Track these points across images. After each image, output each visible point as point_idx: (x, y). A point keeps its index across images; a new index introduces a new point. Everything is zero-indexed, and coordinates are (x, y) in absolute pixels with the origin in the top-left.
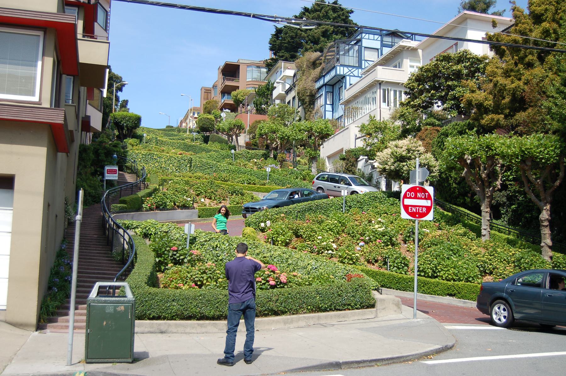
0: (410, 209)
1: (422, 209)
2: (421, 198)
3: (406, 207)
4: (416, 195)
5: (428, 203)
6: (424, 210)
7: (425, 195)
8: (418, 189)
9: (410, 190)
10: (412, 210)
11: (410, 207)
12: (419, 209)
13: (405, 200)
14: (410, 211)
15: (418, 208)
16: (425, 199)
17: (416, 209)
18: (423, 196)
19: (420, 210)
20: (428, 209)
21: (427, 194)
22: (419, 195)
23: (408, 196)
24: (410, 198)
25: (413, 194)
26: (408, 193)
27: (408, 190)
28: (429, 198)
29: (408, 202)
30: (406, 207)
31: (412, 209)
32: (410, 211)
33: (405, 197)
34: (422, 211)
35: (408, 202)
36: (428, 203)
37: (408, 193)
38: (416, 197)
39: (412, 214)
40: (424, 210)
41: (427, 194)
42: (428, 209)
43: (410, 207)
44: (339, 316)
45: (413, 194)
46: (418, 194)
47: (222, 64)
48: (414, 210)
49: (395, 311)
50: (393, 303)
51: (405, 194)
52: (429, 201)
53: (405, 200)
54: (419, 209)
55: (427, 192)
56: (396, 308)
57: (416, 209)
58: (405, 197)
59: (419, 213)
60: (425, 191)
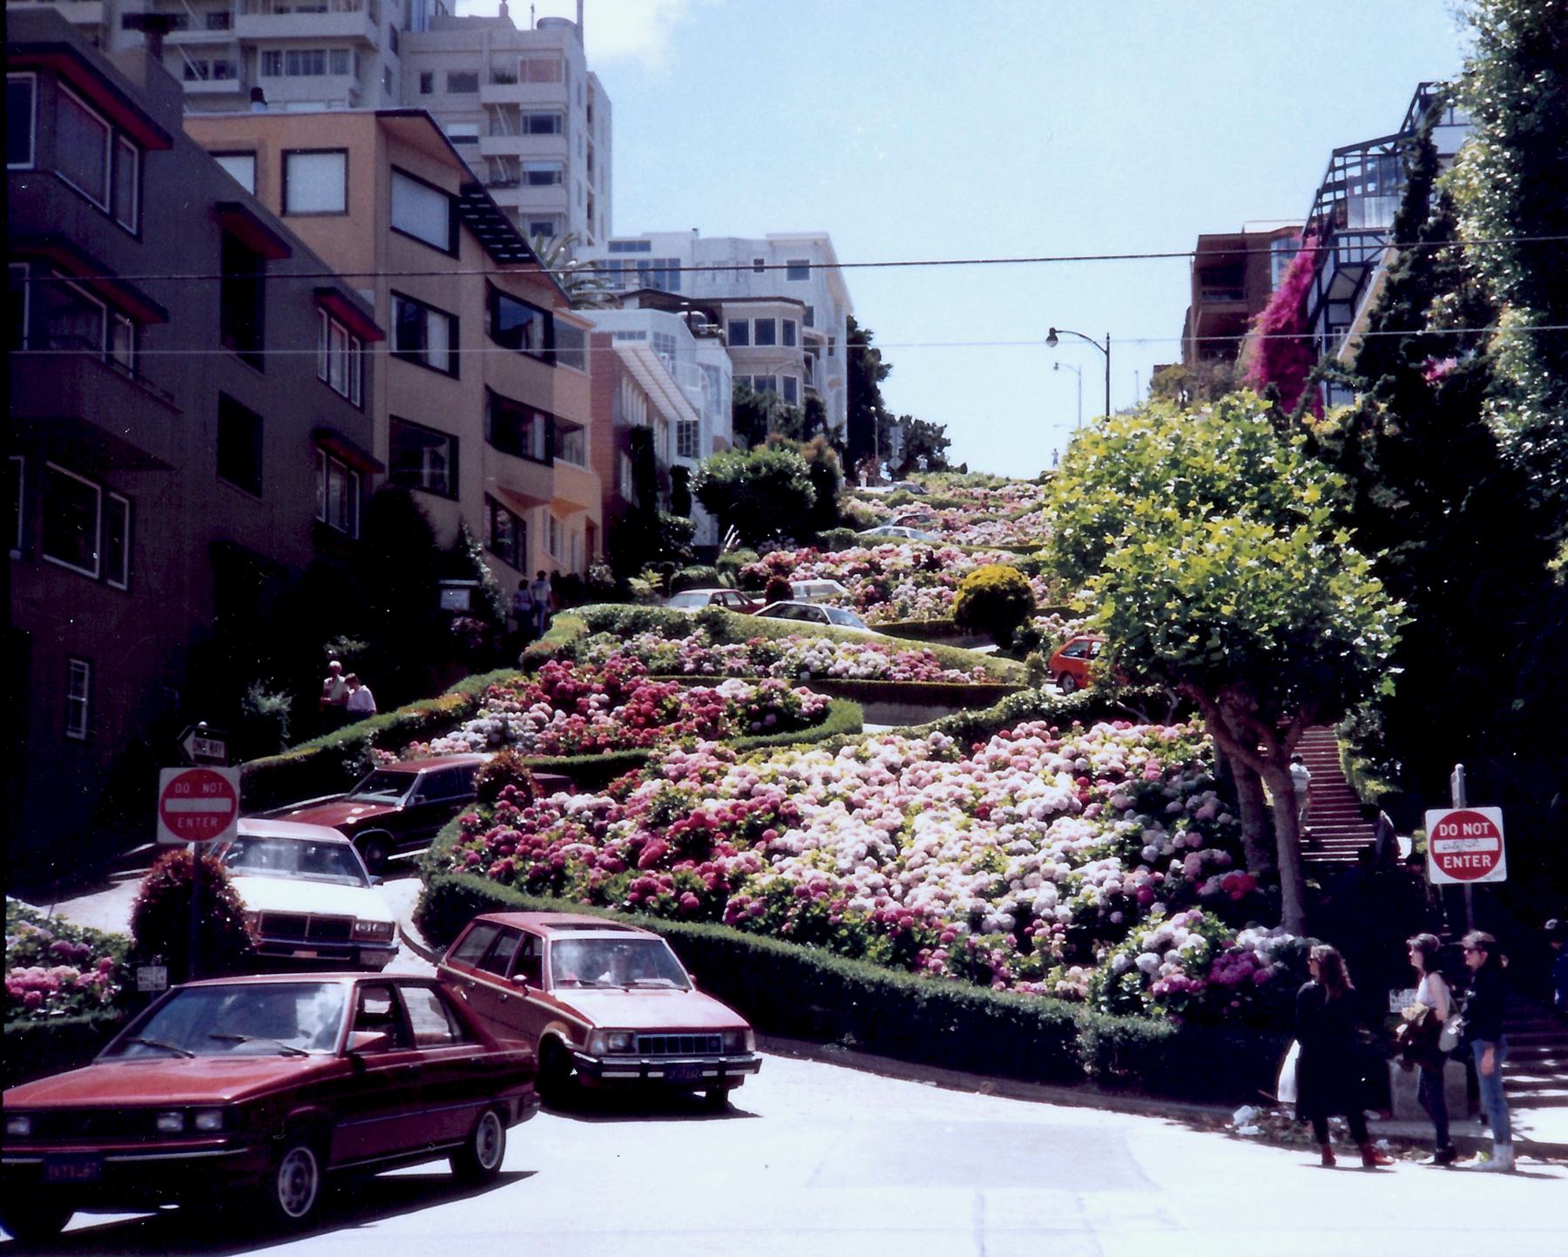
2: (1474, 836)
4: (1460, 830)
5: (1491, 844)
6: (1486, 860)
9: (1447, 820)
12: (1471, 860)
15: (1467, 858)
16: (1483, 836)
17: (1464, 861)
18: (1477, 830)
19: (1475, 861)
20: (1494, 856)
21: (1486, 824)
22: (1467, 828)
24: (1448, 837)
28: (1492, 832)
30: (1439, 858)
33: (1436, 835)
36: (1491, 844)
38: (1461, 836)
48: (1458, 862)
54: (1471, 860)
57: (1464, 861)
58: (1436, 835)
60: (1482, 819)
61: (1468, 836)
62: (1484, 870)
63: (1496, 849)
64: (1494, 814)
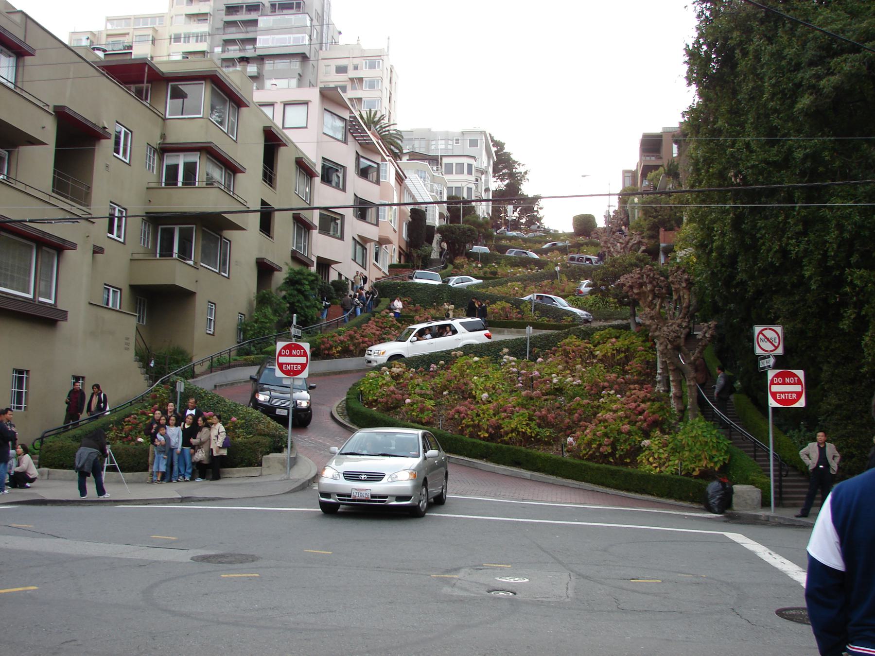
2: (296, 356)
3: (281, 366)
4: (291, 352)
5: (303, 360)
6: (299, 367)
8: (293, 346)
9: (285, 348)
13: (280, 358)
16: (300, 356)
20: (304, 366)
21: (302, 351)
22: (294, 352)
24: (285, 355)
27: (283, 348)
28: (305, 355)
29: (282, 360)
30: (281, 366)
33: (280, 355)
35: (282, 360)
36: (303, 360)
38: (291, 355)
39: (286, 372)
40: (299, 367)
42: (304, 366)
47: (640, 137)
48: (288, 367)
50: (279, 462)
51: (281, 351)
52: (305, 358)
53: (280, 357)
55: (303, 348)
56: (281, 467)
60: (301, 348)
61: (294, 356)
62: (299, 372)
63: (305, 362)
64: (306, 346)
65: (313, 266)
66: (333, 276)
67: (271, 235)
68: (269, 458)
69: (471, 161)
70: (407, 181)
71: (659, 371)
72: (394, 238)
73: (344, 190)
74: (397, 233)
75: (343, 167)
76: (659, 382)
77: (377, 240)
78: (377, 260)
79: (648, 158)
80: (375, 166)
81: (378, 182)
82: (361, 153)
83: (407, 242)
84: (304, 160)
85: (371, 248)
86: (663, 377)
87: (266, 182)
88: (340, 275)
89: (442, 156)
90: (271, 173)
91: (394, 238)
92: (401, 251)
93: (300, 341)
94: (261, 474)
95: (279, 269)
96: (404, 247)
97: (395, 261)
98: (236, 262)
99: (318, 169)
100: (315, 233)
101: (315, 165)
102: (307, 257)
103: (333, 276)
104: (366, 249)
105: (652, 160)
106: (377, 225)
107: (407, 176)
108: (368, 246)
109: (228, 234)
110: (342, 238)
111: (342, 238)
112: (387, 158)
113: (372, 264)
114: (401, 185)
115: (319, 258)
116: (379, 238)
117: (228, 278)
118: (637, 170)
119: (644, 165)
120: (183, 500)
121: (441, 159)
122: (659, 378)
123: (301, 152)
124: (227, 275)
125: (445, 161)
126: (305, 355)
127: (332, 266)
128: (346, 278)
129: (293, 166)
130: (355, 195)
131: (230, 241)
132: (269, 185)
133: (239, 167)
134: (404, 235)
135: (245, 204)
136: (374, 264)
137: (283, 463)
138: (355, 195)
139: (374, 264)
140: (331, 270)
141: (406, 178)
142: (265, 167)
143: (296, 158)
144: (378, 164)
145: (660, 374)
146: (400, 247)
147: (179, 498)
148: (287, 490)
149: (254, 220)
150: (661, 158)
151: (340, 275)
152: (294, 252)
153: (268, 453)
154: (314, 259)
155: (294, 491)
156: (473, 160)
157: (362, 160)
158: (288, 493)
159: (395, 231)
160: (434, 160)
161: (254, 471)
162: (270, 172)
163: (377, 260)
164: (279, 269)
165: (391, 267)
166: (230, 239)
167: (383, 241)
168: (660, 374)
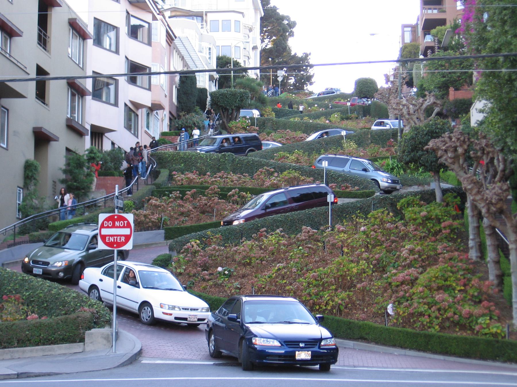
0: (107, 239)
1: (120, 238)
2: (120, 227)
5: (127, 231)
6: (123, 239)
7: (124, 223)
8: (116, 217)
9: (107, 219)
10: (109, 240)
11: (107, 237)
12: (117, 239)
13: (103, 230)
14: (107, 241)
15: (115, 237)
16: (124, 227)
17: (114, 239)
18: (122, 224)
19: (118, 239)
20: (127, 238)
21: (126, 222)
22: (117, 224)
23: (105, 226)
24: (108, 227)
25: (110, 224)
26: (105, 222)
28: (129, 226)
29: (105, 232)
30: (103, 238)
31: (109, 238)
32: (107, 241)
33: (102, 226)
34: (120, 240)
36: (127, 231)
37: (105, 222)
38: (114, 226)
41: (126, 222)
42: (127, 238)
43: (107, 237)
44: (43, 350)
45: (110, 224)
46: (116, 222)
48: (112, 239)
49: (105, 345)
52: (129, 230)
54: (117, 239)
55: (126, 220)
56: (105, 342)
57: (114, 239)
58: (102, 226)
59: (117, 243)
60: (124, 219)
61: (117, 227)
64: (130, 217)
65: (88, 135)
66: (107, 147)
67: (46, 102)
68: (92, 334)
69: (239, 17)
70: (176, 41)
71: (471, 237)
72: (166, 103)
73: (117, 52)
74: (168, 97)
75: (116, 27)
76: (472, 248)
77: (150, 106)
78: (148, 127)
79: (430, 11)
80: (146, 25)
81: (149, 44)
82: (131, 13)
83: (177, 107)
84: (77, 21)
85: (142, 113)
86: (476, 243)
87: (41, 46)
88: (113, 144)
89: (206, 13)
90: (46, 36)
91: (166, 103)
92: (171, 117)
93: (123, 213)
94: (84, 349)
95: (56, 140)
96: (174, 113)
97: (166, 129)
98: (14, 131)
99: (91, 30)
100: (89, 98)
101: (87, 26)
102: (81, 125)
103: (107, 147)
104: (137, 115)
105: (433, 13)
106: (149, 89)
107: (176, 35)
108: (139, 112)
109: (7, 102)
110: (116, 104)
111: (116, 104)
112: (158, 17)
113: (143, 133)
114: (170, 46)
115: (92, 126)
116: (152, 104)
117: (7, 149)
118: (417, 24)
119: (426, 20)
120: (19, 376)
121: (206, 15)
122: (471, 243)
123: (75, 13)
124: (5, 146)
125: (210, 17)
126: (129, 226)
127: (106, 134)
128: (119, 147)
129: (67, 27)
130: (126, 57)
131: (8, 110)
132: (43, 48)
133: (17, 31)
134: (175, 100)
135: (25, 69)
136: (146, 132)
137: (108, 338)
138: (126, 57)
139: (146, 132)
140: (105, 139)
141: (176, 37)
142: (39, 30)
143: (69, 19)
144: (149, 23)
145: (472, 240)
146: (170, 113)
147: (15, 374)
148: (117, 364)
149: (30, 89)
150: (445, 12)
151: (113, 144)
152: (68, 120)
153: (90, 329)
154: (88, 128)
155: (123, 365)
156: (241, 15)
157: (132, 19)
158: (118, 366)
159: (166, 96)
160: (200, 16)
161: (77, 347)
162: (44, 34)
163: (148, 127)
164: (56, 140)
165: (163, 134)
166: (7, 107)
167: (155, 107)
168: (472, 240)
